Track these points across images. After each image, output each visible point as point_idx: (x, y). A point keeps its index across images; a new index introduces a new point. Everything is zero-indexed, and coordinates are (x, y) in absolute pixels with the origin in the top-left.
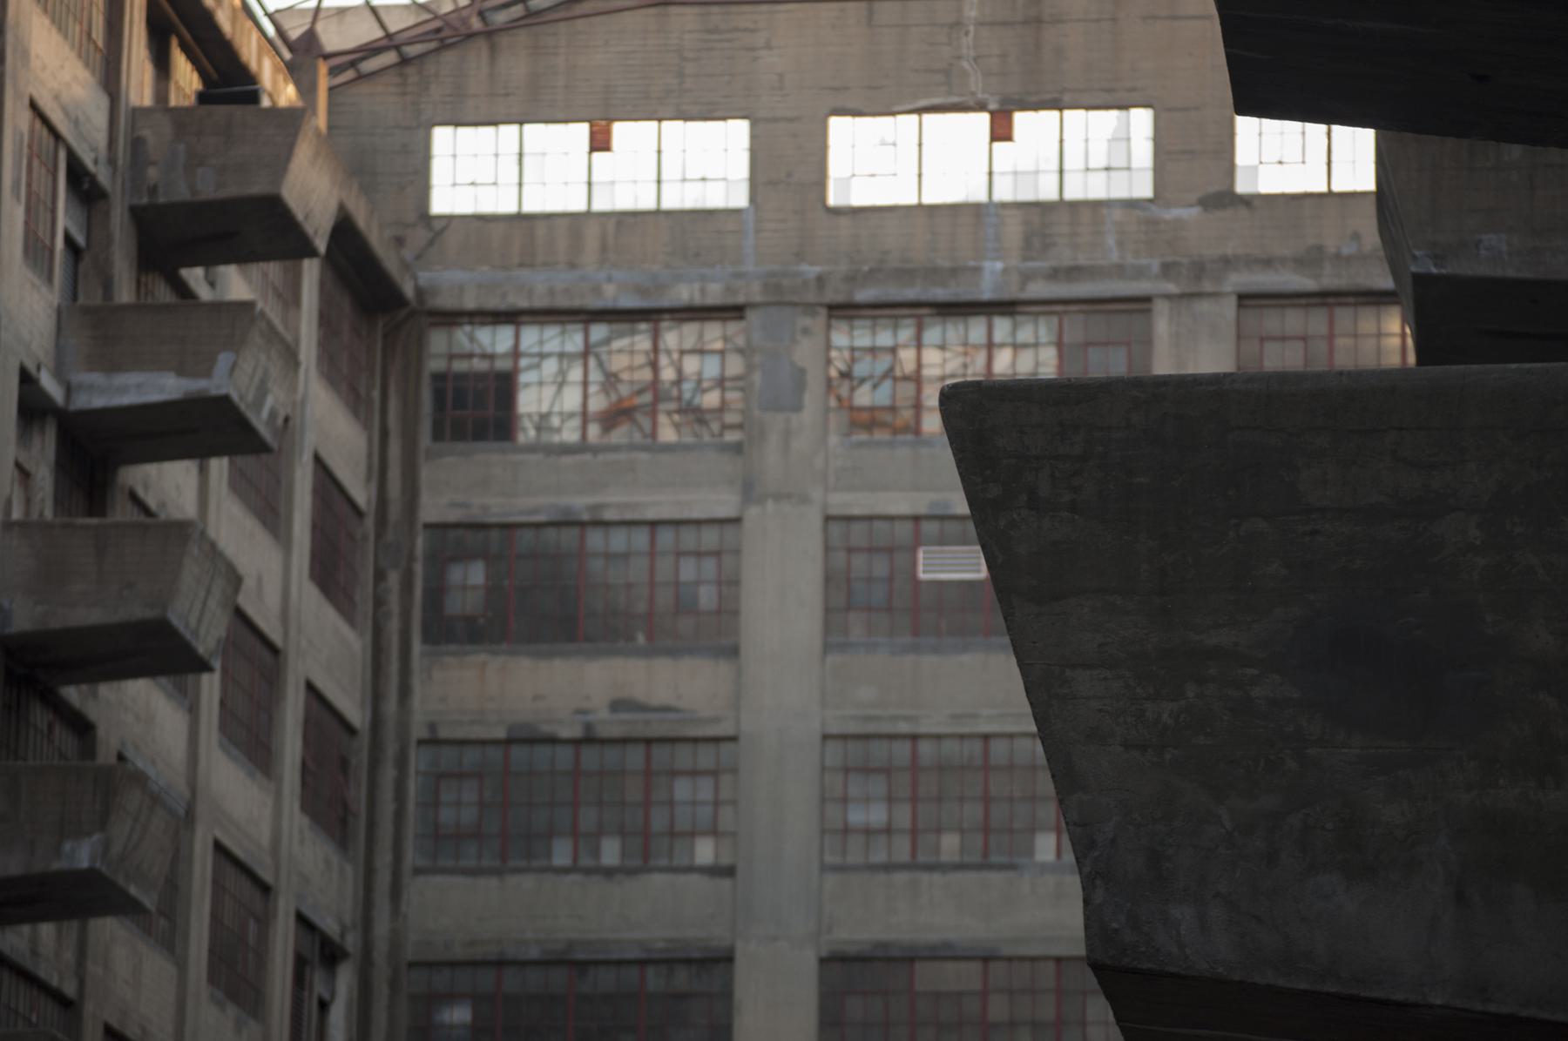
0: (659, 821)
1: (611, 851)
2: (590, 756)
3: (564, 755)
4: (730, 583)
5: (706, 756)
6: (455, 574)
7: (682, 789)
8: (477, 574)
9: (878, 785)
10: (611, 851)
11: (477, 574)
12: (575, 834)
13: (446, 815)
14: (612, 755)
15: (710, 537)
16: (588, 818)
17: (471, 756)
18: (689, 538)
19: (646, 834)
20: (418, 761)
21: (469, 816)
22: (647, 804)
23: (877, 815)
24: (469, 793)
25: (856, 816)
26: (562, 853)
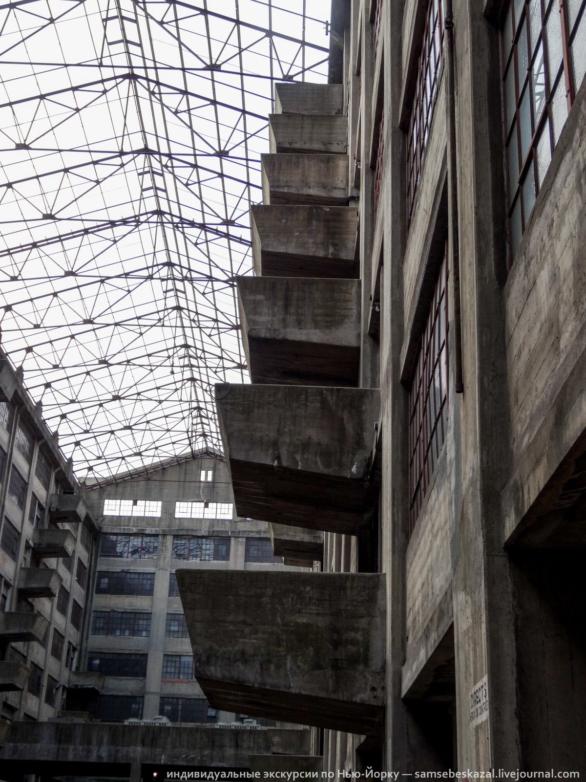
0: (136, 628)
1: (127, 633)
2: (125, 616)
4: (152, 585)
5: (146, 616)
6: (102, 580)
7: (141, 622)
8: (106, 581)
9: (176, 623)
11: (106, 581)
12: (121, 629)
13: (97, 625)
14: (129, 616)
16: (123, 626)
18: (145, 576)
19: (134, 630)
20: (93, 614)
21: (101, 625)
22: (134, 624)
23: (176, 629)
24: (102, 621)
25: (172, 628)
26: (118, 633)
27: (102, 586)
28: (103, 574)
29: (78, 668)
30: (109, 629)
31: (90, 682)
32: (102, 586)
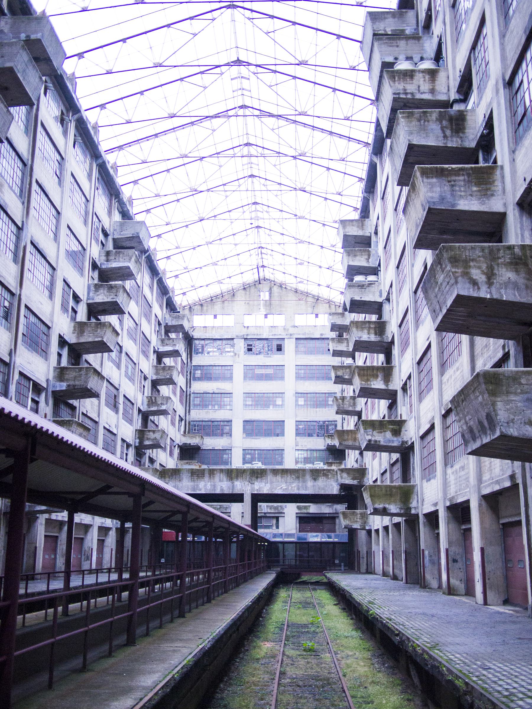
0: (222, 403)
1: (216, 407)
2: (214, 395)
3: (210, 395)
5: (228, 395)
6: (197, 372)
7: (225, 399)
9: (250, 399)
10: (216, 407)
11: (199, 372)
12: (212, 405)
13: (195, 402)
14: (217, 395)
15: (229, 368)
16: (213, 403)
17: (199, 395)
18: (226, 368)
19: (221, 405)
20: (192, 395)
21: (198, 402)
22: (221, 401)
23: (250, 403)
24: (198, 399)
25: (248, 403)
26: (210, 407)
27: (197, 376)
28: (197, 367)
29: (185, 432)
30: (204, 405)
31: (194, 441)
32: (197, 376)
